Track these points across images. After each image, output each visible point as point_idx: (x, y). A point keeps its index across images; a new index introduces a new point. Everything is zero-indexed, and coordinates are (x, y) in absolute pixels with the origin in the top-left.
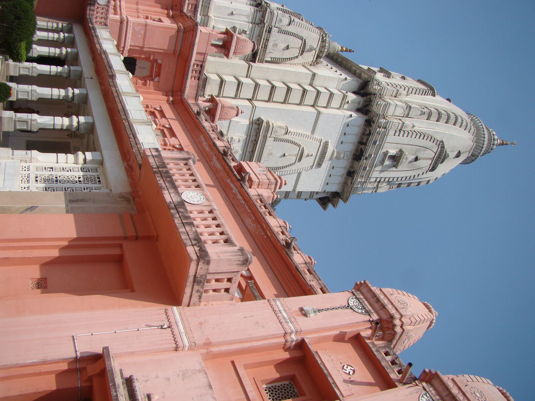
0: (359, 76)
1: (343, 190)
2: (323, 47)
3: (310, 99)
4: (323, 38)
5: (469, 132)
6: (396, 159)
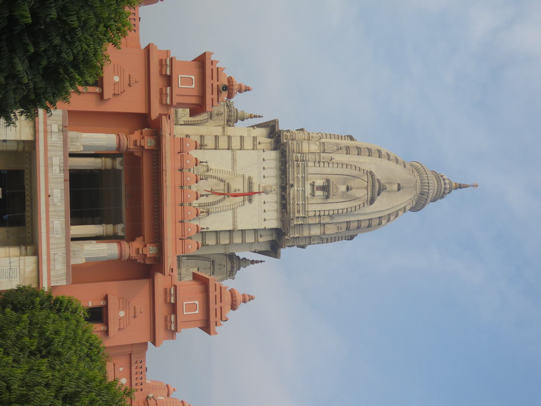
0: (268, 126)
1: (284, 225)
2: (230, 111)
3: (223, 142)
4: (227, 105)
5: (405, 166)
6: (325, 188)
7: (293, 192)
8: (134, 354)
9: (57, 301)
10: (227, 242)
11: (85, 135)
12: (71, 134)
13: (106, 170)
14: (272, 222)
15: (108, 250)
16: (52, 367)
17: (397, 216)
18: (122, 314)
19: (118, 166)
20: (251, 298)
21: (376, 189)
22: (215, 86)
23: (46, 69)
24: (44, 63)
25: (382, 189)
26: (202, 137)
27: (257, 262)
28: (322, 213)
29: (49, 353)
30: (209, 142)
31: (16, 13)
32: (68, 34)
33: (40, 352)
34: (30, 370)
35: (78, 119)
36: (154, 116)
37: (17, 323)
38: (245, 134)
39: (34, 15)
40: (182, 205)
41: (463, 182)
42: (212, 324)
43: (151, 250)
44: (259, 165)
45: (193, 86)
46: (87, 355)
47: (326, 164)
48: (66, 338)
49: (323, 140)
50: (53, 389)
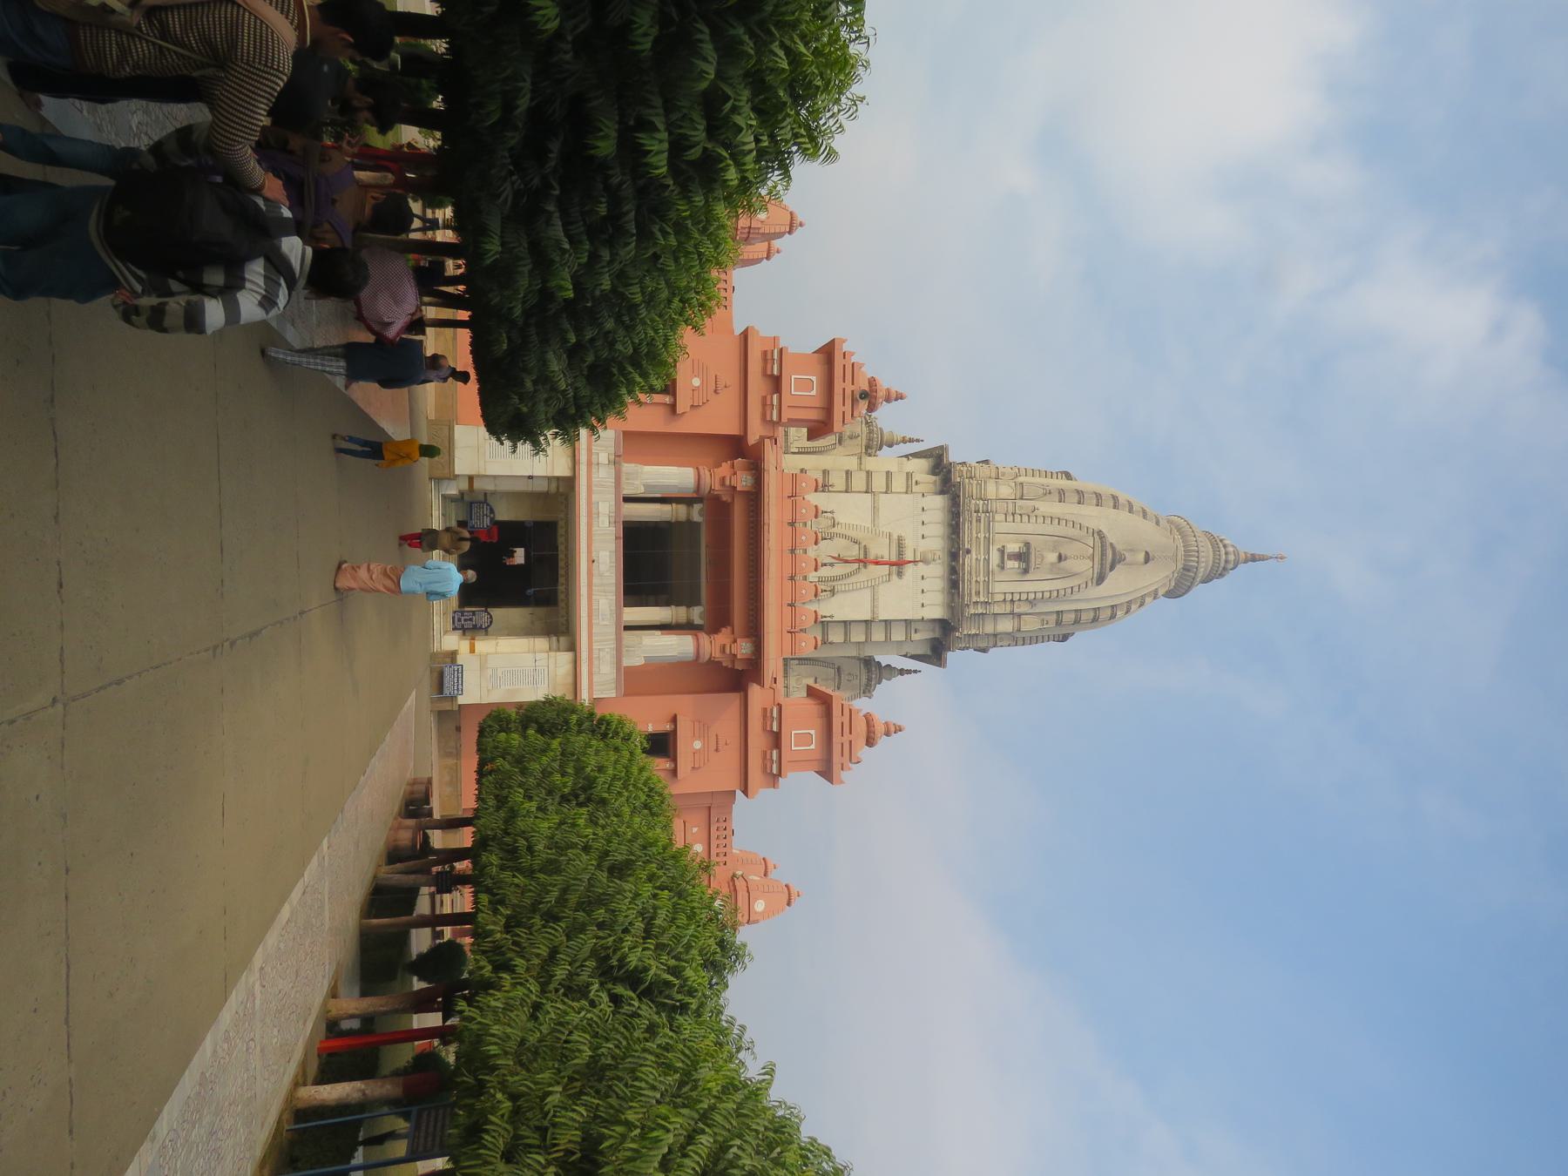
0: (931, 456)
2: (871, 432)
3: (859, 482)
5: (1157, 523)
6: (1023, 557)
7: (969, 562)
8: (715, 807)
9: (601, 721)
10: (862, 639)
11: (647, 468)
12: (627, 467)
13: (678, 523)
14: (936, 610)
15: (678, 646)
16: (593, 821)
17: (1142, 605)
18: (697, 745)
19: (696, 518)
20: (899, 729)
21: (1109, 559)
22: (848, 393)
23: (592, 367)
24: (590, 359)
25: (1117, 560)
26: (825, 473)
27: (909, 672)
28: (1016, 597)
29: (589, 800)
30: (838, 481)
31: (553, 284)
32: (627, 313)
33: (577, 797)
34: (562, 823)
35: (637, 444)
36: (752, 439)
37: (544, 751)
38: (894, 469)
39: (577, 286)
40: (792, 578)
41: (1257, 552)
42: (836, 767)
43: (743, 648)
44: (916, 518)
45: (814, 393)
46: (646, 806)
47: (1025, 518)
48: (614, 778)
49: (1021, 479)
50: (595, 855)
